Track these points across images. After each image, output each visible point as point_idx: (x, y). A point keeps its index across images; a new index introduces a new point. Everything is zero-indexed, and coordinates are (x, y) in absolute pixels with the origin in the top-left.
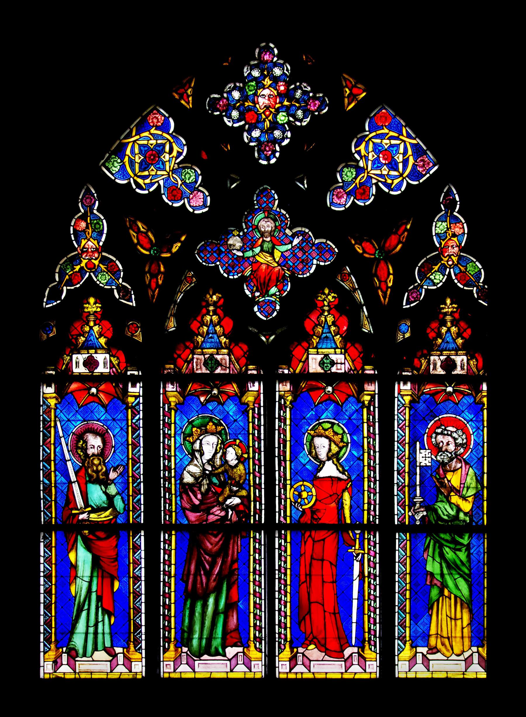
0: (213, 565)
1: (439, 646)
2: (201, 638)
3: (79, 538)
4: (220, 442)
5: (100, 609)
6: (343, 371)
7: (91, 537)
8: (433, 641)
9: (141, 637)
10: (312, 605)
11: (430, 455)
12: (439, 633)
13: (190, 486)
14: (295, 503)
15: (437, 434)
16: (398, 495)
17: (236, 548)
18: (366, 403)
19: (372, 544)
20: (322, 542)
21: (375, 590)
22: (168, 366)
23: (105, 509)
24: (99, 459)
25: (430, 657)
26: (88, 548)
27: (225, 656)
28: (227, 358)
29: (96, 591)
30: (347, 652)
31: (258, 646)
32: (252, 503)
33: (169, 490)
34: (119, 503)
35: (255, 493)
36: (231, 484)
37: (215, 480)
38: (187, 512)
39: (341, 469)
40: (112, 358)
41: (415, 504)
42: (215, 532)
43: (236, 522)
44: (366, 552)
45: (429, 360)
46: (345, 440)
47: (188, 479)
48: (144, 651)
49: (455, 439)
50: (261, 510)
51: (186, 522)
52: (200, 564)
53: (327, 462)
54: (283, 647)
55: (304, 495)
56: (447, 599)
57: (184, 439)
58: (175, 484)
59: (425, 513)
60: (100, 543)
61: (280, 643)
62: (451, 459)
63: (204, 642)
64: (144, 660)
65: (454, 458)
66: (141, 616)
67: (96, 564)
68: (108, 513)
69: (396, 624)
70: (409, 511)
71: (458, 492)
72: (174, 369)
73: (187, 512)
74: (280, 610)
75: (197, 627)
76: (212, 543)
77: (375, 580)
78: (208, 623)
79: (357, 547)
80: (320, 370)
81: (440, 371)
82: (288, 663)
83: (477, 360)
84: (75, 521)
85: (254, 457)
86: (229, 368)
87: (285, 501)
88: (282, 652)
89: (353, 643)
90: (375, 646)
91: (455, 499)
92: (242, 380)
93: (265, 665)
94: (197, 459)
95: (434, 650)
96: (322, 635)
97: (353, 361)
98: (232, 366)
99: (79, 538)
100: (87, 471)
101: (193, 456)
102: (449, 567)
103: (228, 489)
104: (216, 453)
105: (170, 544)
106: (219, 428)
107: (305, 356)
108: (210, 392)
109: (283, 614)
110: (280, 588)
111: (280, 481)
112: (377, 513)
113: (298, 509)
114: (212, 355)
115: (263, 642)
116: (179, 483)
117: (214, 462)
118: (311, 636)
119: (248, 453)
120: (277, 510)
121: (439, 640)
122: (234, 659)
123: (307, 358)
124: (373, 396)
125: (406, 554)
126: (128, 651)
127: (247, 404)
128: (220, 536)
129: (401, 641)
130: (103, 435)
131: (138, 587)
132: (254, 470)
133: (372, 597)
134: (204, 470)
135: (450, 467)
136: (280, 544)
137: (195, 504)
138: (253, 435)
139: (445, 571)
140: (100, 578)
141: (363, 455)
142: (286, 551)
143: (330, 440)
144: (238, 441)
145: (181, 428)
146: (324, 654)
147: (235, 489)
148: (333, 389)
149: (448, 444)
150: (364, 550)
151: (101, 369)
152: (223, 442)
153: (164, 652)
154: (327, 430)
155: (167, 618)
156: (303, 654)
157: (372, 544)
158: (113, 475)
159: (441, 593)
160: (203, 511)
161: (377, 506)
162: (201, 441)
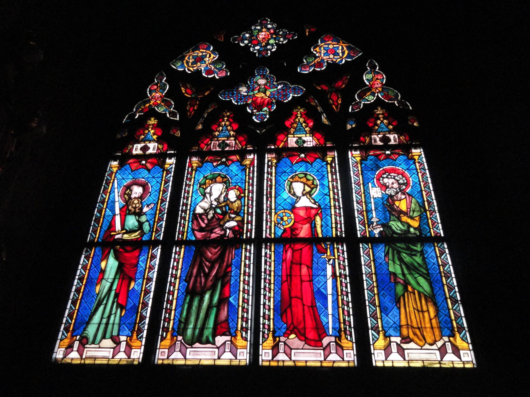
0: (211, 269)
1: (411, 336)
2: (194, 328)
3: (112, 251)
4: (225, 187)
5: (115, 304)
6: (312, 145)
7: (121, 250)
8: (405, 332)
9: (144, 327)
10: (293, 300)
11: (380, 190)
12: (410, 323)
13: (200, 215)
14: (278, 224)
15: (383, 178)
16: (358, 217)
17: (231, 256)
18: (329, 162)
19: (341, 251)
20: (300, 251)
21: (346, 287)
22: (194, 148)
23: (135, 231)
24: (138, 200)
25: (404, 346)
26: (117, 258)
27: (214, 344)
28: (234, 142)
29: (116, 290)
30: (325, 341)
31: (244, 335)
32: (245, 225)
33: (184, 218)
34: (146, 227)
35: (248, 219)
36: (230, 213)
37: (219, 211)
38: (196, 232)
39: (313, 201)
40: (159, 146)
41: (372, 223)
42: (215, 246)
43: (231, 238)
44: (336, 257)
45: (371, 138)
46: (315, 183)
47: (199, 210)
48: (144, 340)
49: (397, 181)
50: (251, 229)
51: (194, 239)
52: (201, 268)
53: (302, 197)
54: (266, 336)
55: (285, 218)
56: (412, 294)
57: (200, 187)
58: (189, 214)
59: (382, 229)
60: (127, 255)
61: (264, 333)
62: (397, 193)
63: (197, 331)
64: (143, 347)
65: (398, 193)
66: (147, 309)
67: (120, 269)
68: (137, 233)
69: (368, 316)
70: (369, 227)
71: (406, 214)
72: (198, 149)
73: (196, 232)
74: (264, 304)
75: (193, 319)
76: (211, 253)
77: (346, 279)
78: (202, 315)
79: (329, 254)
80: (295, 145)
81: (379, 143)
82: (270, 351)
83: (404, 136)
84: (111, 240)
85: (248, 196)
86: (235, 147)
87: (271, 223)
88: (265, 340)
89: (331, 333)
90: (351, 336)
91: (404, 219)
92: (243, 153)
93: (250, 353)
94: (207, 198)
95: (406, 340)
96: (302, 326)
97: (318, 140)
98: (236, 146)
99: (112, 251)
100: (128, 207)
101: (204, 196)
102: (408, 268)
103: (227, 216)
104: (221, 194)
105: (179, 256)
106: (225, 180)
107: (285, 139)
108: (221, 160)
109: (267, 307)
110: (265, 286)
111: (267, 210)
112: (343, 230)
113: (280, 228)
114: (224, 141)
115: (249, 331)
116: (193, 214)
117: (219, 200)
118: (292, 326)
119: (245, 194)
120: (264, 229)
121: (410, 331)
122: (222, 347)
123: (287, 140)
124: (334, 158)
125: (370, 259)
126: (131, 340)
127: (246, 165)
128: (219, 248)
129: (375, 331)
130: (144, 186)
131: (149, 286)
132: (248, 203)
133: (344, 293)
134: (212, 204)
135: (397, 198)
136: (266, 253)
137: (202, 227)
138: (249, 182)
139: (406, 272)
140: (121, 280)
141: (329, 192)
142: (270, 258)
143: (304, 184)
144: (237, 187)
145: (198, 180)
146: (304, 343)
147: (233, 216)
148: (305, 155)
149: (393, 184)
150: (334, 256)
151: (150, 151)
152: (226, 188)
153: (161, 341)
154: (302, 178)
155: (168, 311)
156: (285, 343)
157: (341, 251)
158: (145, 209)
159: (406, 289)
160: (208, 231)
161: (343, 225)
162: (211, 187)
